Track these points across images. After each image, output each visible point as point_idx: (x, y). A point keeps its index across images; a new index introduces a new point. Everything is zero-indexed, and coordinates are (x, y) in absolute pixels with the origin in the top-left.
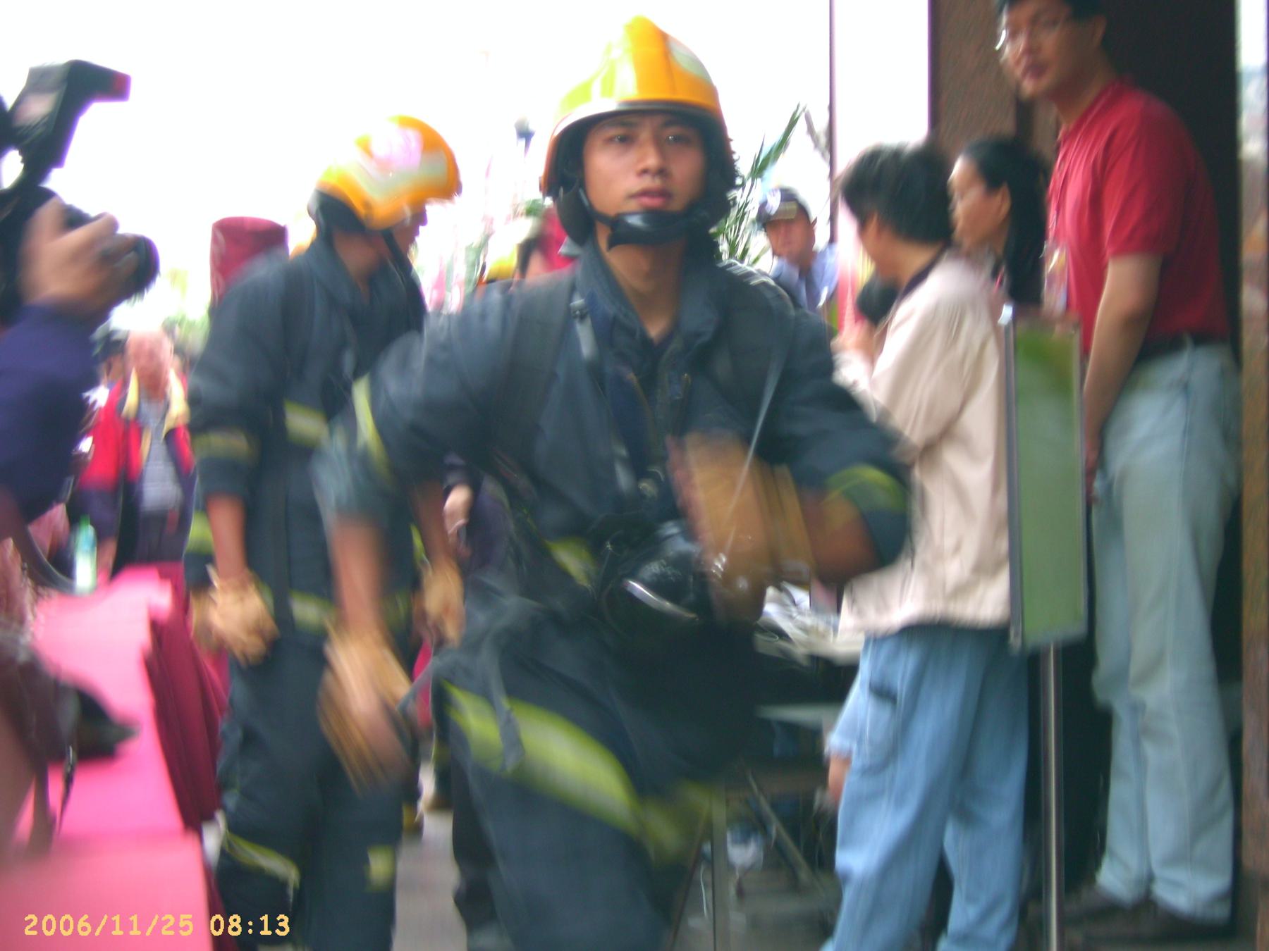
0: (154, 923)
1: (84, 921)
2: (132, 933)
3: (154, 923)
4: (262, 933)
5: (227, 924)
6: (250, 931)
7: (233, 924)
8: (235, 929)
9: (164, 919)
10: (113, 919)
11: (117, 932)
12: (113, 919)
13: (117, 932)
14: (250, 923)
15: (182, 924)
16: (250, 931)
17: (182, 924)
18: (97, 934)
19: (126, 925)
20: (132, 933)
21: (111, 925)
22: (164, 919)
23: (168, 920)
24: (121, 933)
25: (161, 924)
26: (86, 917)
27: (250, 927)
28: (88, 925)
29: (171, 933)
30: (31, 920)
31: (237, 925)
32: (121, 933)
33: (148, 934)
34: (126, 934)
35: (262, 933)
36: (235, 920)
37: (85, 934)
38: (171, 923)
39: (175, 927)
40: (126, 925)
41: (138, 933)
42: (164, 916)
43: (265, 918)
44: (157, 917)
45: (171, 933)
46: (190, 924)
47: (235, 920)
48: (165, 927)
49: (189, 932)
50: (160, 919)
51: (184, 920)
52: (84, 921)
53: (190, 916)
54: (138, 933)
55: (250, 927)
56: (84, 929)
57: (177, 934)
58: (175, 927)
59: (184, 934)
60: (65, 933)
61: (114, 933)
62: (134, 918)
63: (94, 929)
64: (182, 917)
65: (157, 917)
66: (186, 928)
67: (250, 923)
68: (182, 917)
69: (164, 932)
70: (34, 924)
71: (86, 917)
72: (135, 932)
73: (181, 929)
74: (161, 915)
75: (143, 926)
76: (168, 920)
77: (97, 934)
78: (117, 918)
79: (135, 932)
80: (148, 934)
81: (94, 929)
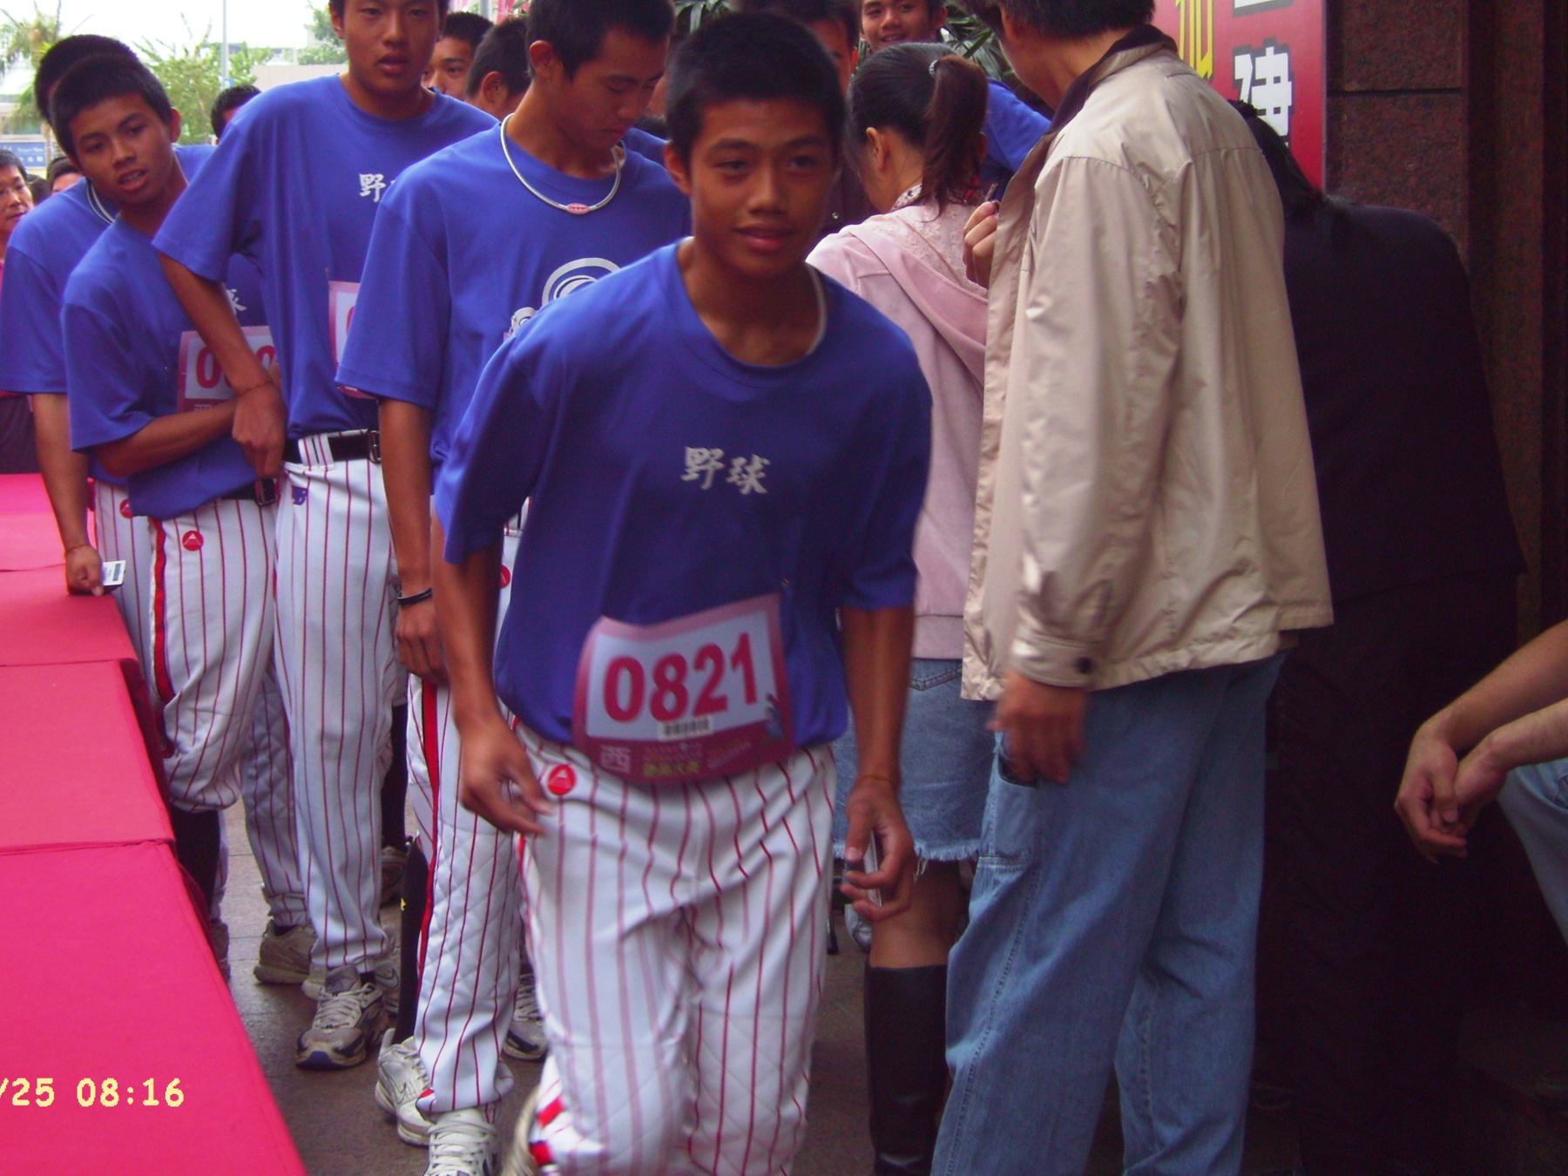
4: (146, 1103)
5: (99, 1091)
6: (130, 1101)
7: (106, 1091)
8: (110, 1098)
9: (15, 1084)
14: (130, 1090)
15: (39, 1091)
16: (130, 1101)
17: (39, 1091)
22: (15, 1084)
23: (21, 1086)
25: (11, 1090)
27: (131, 1095)
29: (26, 1103)
35: (146, 1103)
36: (110, 1086)
38: (25, 1090)
39: (31, 1095)
42: (15, 1080)
43: (150, 1083)
44: (6, 1081)
45: (26, 1103)
47: (110, 1086)
50: (9, 1086)
51: (42, 1085)
53: (50, 1081)
57: (33, 1102)
58: (31, 1095)
64: (40, 1081)
65: (6, 1081)
66: (45, 1096)
67: (130, 1090)
68: (40, 1081)
69: (16, 1102)
73: (39, 1097)
74: (12, 1080)
76: (21, 1086)
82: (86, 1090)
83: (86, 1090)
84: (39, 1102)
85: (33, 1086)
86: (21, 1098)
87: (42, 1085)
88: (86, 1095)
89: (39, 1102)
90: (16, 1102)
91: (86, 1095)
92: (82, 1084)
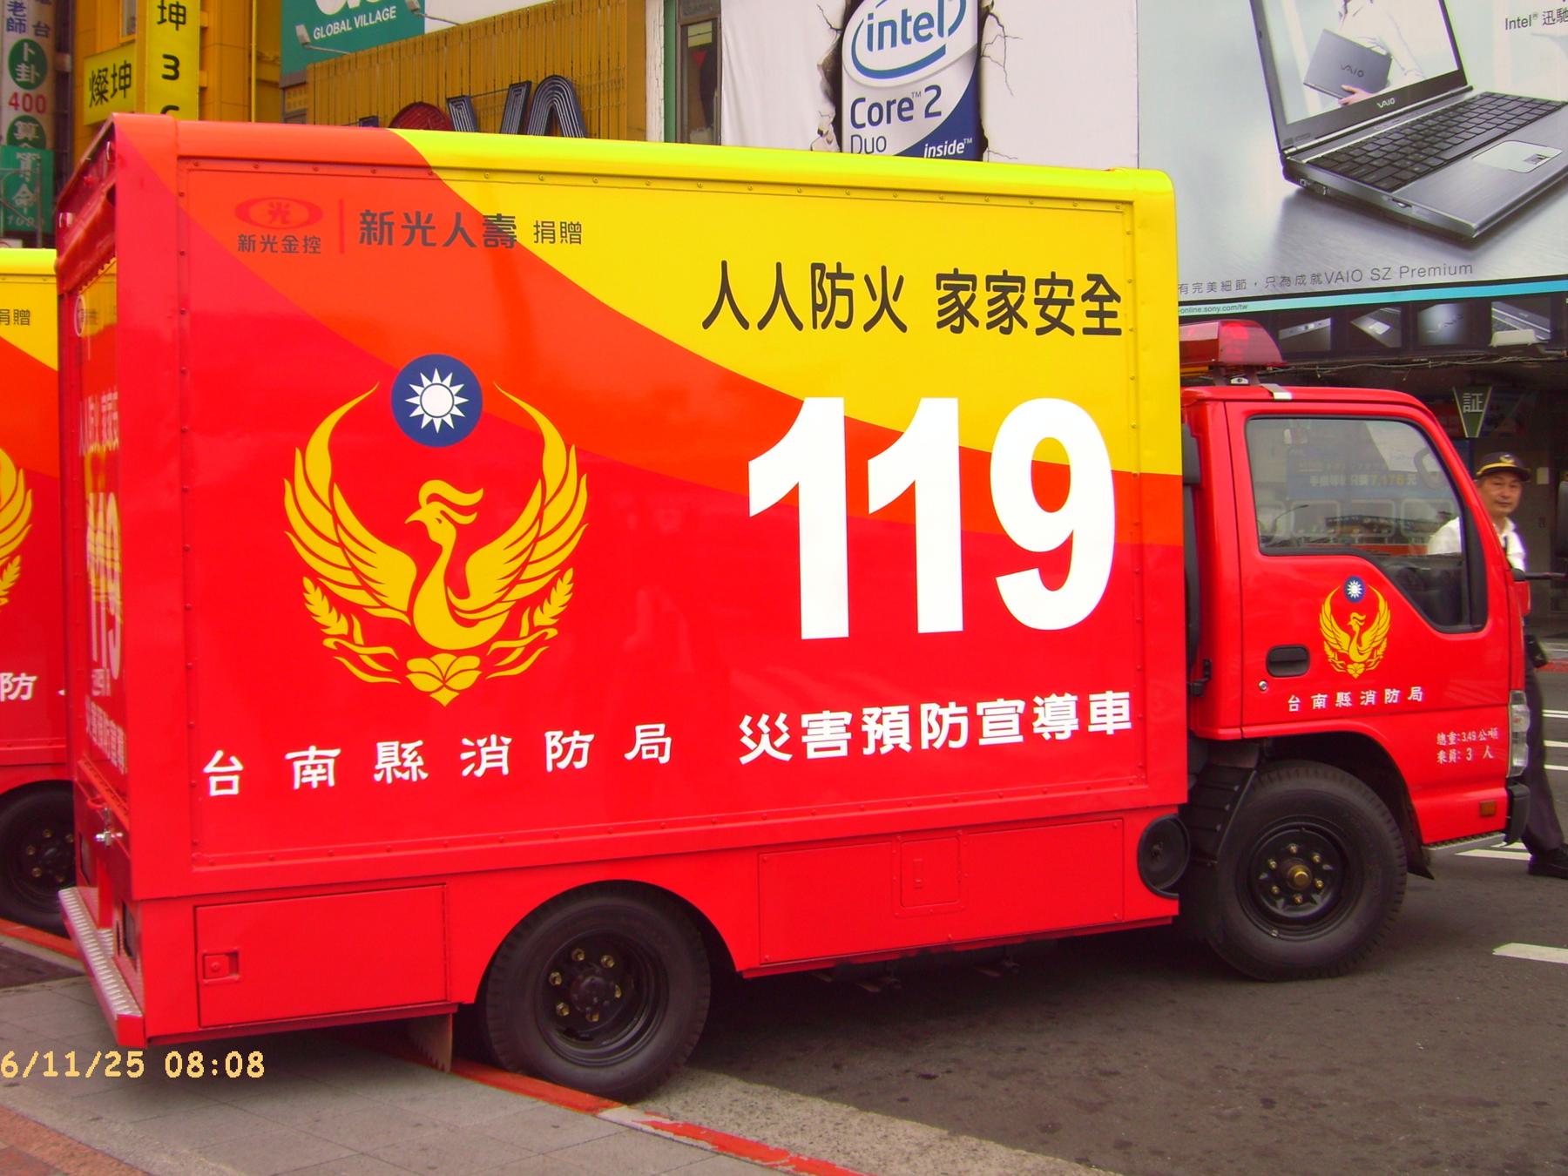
0: (96, 1061)
1: (9, 1060)
2: (68, 1074)
3: (96, 1061)
7: (192, 1063)
8: (195, 1069)
9: (107, 1056)
10: (45, 1057)
12: (45, 1057)
13: (51, 1073)
14: (215, 1062)
15: (130, 1063)
16: (215, 1072)
17: (130, 1063)
18: (25, 1074)
19: (62, 1065)
20: (68, 1074)
21: (42, 1064)
22: (107, 1056)
23: (113, 1059)
24: (55, 1074)
25: (105, 1062)
26: (11, 1054)
27: (215, 1067)
28: (14, 1065)
29: (118, 1074)
31: (198, 1064)
32: (55, 1074)
33: (88, 1075)
34: (62, 1075)
36: (196, 1058)
38: (117, 1062)
40: (62, 1065)
41: (77, 1074)
42: (108, 1053)
45: (118, 1074)
46: (140, 1063)
48: (110, 1067)
49: (139, 1073)
50: (102, 1058)
51: (133, 1058)
52: (9, 1060)
53: (140, 1054)
54: (77, 1074)
55: (215, 1067)
56: (9, 1069)
57: (125, 1075)
58: (122, 1067)
59: (131, 1074)
61: (46, 1074)
62: (71, 1056)
63: (22, 1068)
64: (131, 1054)
66: (135, 1069)
67: (215, 1062)
69: (108, 1073)
71: (11, 1054)
72: (72, 1073)
73: (130, 1068)
74: (105, 1052)
75: (82, 1065)
76: (113, 1059)
77: (25, 1074)
78: (50, 1056)
80: (88, 1075)
81: (22, 1069)
82: (174, 1061)
83: (174, 1062)
84: (129, 1073)
85: (124, 1058)
86: (112, 1070)
87: (133, 1058)
88: (174, 1067)
89: (129, 1073)
91: (174, 1067)
92: (170, 1056)
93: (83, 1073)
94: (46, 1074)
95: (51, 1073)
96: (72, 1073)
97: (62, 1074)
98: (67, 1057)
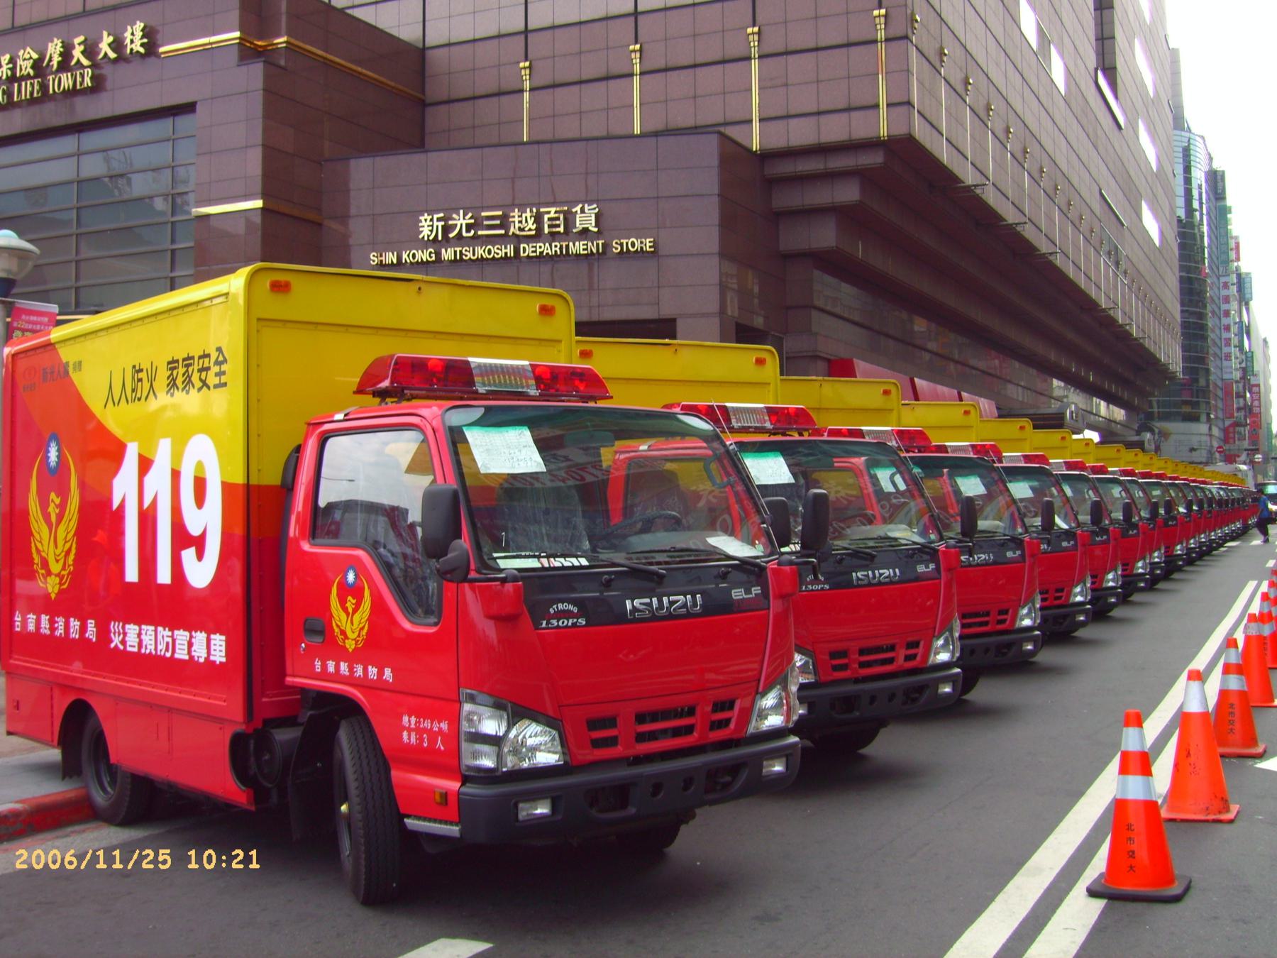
9: (144, 853)
11: (102, 866)
14: (224, 858)
17: (161, 858)
18: (83, 867)
21: (95, 859)
22: (144, 853)
23: (148, 855)
24: (105, 866)
25: (141, 858)
27: (224, 861)
29: (151, 866)
30: (22, 855)
32: (105, 866)
33: (130, 867)
37: (72, 867)
38: (151, 857)
39: (155, 861)
41: (121, 866)
44: (138, 851)
45: (151, 866)
46: (168, 858)
48: (146, 861)
50: (140, 854)
51: (163, 854)
53: (168, 851)
54: (121, 866)
56: (71, 863)
58: (155, 861)
60: (53, 867)
62: (117, 853)
63: (79, 863)
64: (161, 851)
65: (138, 851)
66: (165, 862)
67: (224, 858)
69: (144, 866)
70: (24, 858)
74: (141, 851)
75: (124, 861)
76: (148, 855)
77: (83, 867)
78: (101, 853)
79: (118, 866)
80: (130, 867)
81: (79, 863)
84: (160, 865)
85: (156, 855)
87: (163, 854)
89: (160, 865)
90: (144, 866)
93: (126, 866)
94: (98, 866)
95: (102, 866)
96: (118, 866)
97: (110, 867)
98: (114, 854)
